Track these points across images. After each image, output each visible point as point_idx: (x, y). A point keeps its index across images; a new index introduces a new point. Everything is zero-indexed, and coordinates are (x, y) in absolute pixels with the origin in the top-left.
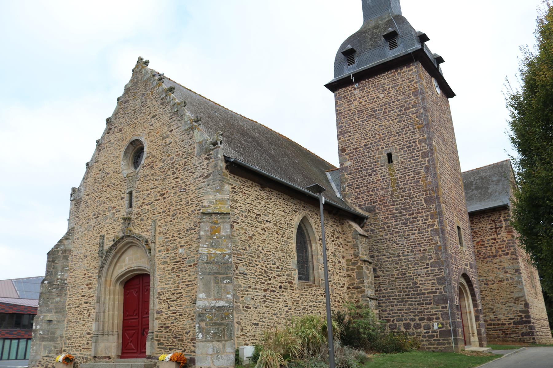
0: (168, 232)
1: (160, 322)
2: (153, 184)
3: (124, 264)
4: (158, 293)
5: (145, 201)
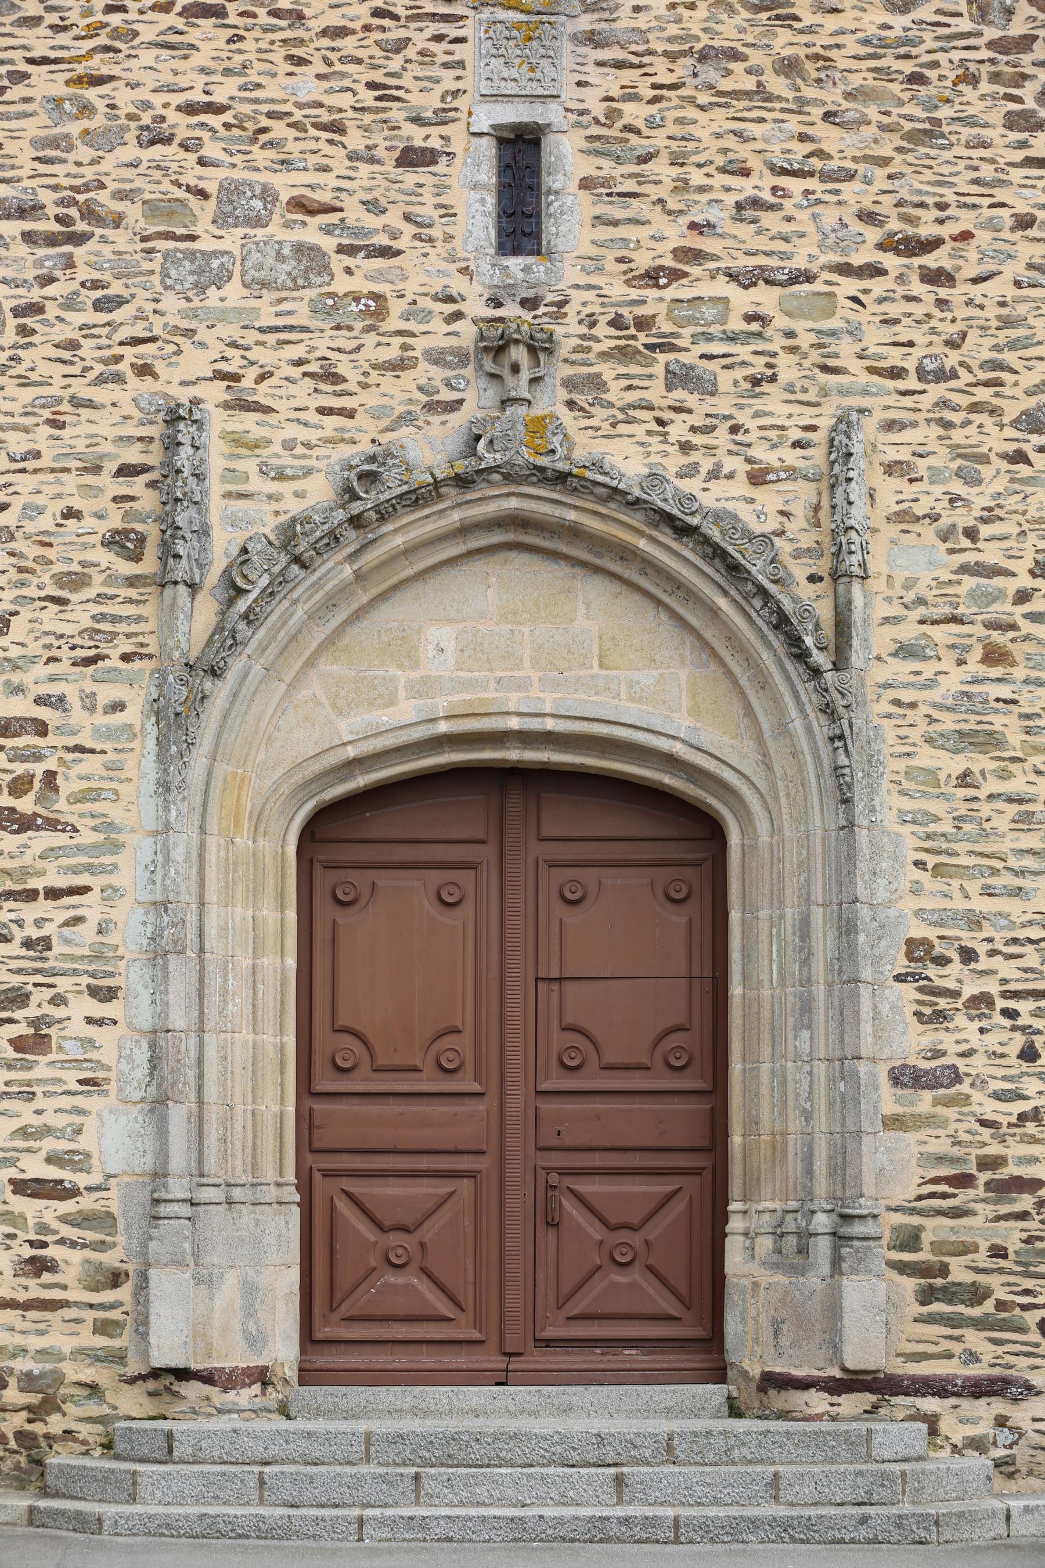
0: (985, 530)
1: (942, 1146)
2: (803, 138)
3: (402, 677)
4: (910, 942)
5: (708, 244)
